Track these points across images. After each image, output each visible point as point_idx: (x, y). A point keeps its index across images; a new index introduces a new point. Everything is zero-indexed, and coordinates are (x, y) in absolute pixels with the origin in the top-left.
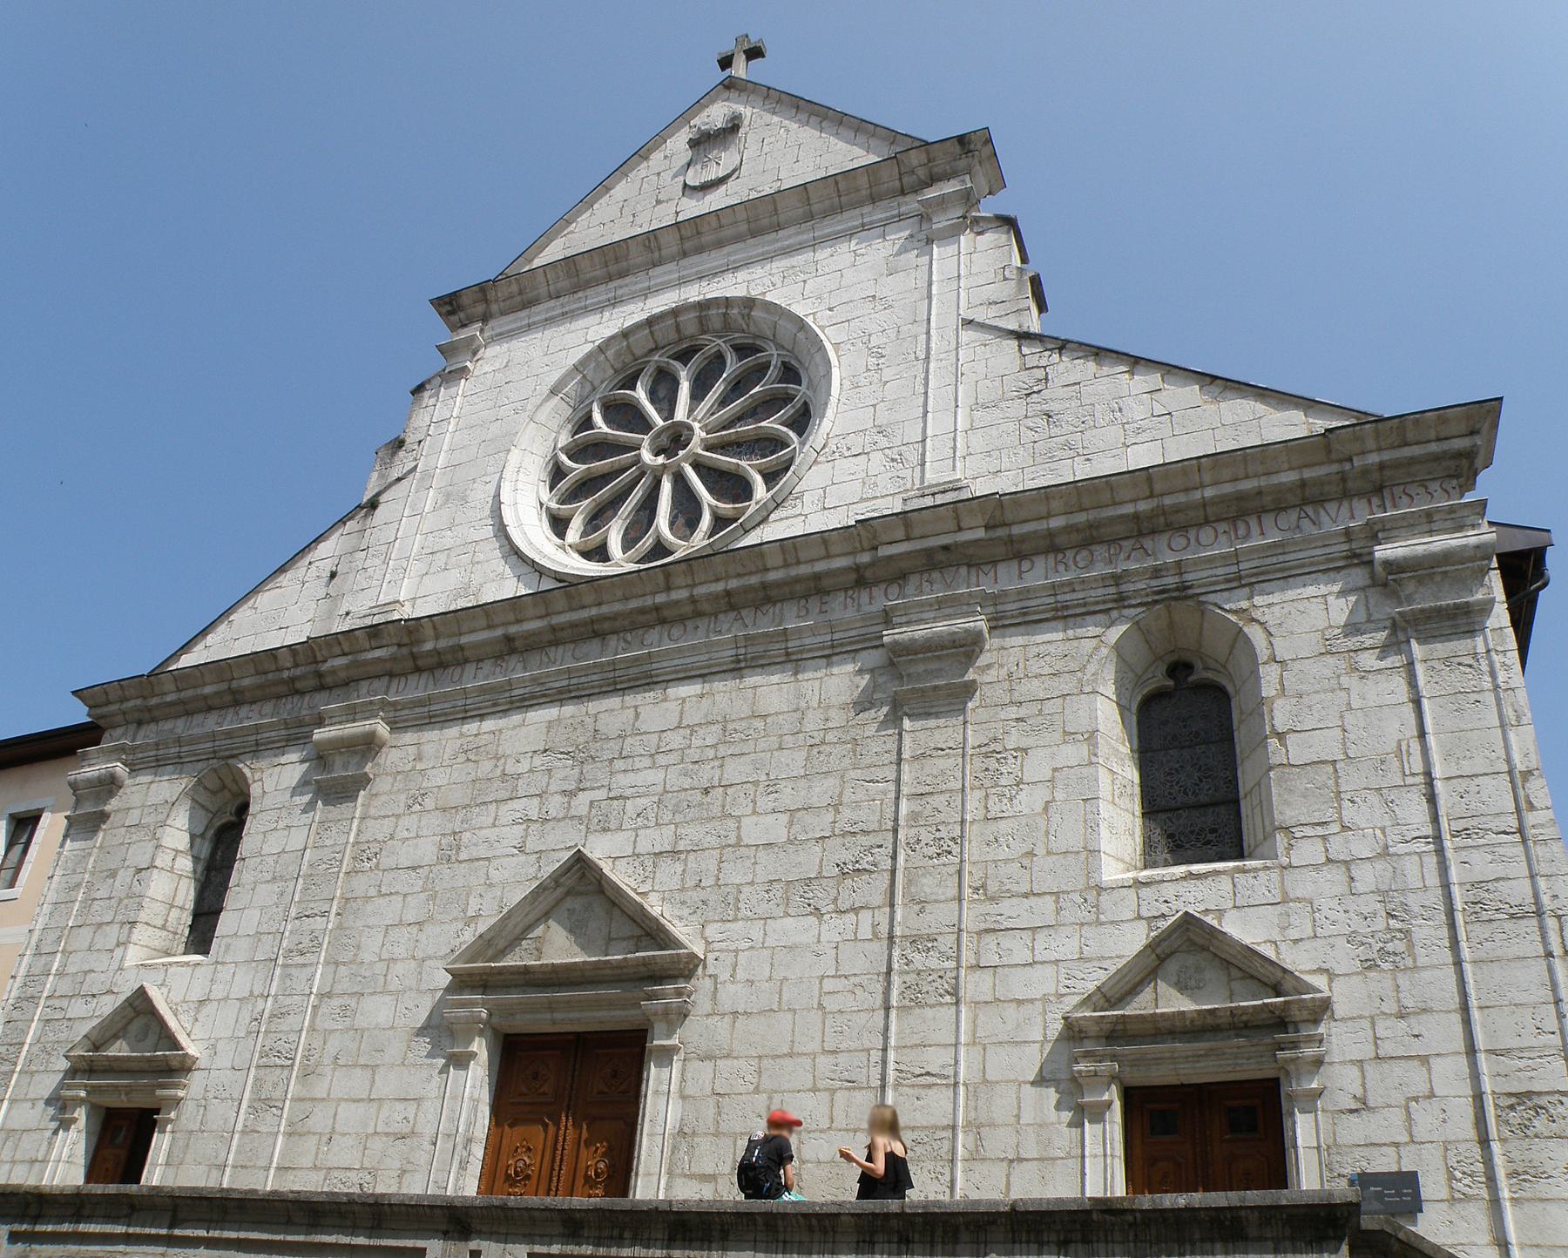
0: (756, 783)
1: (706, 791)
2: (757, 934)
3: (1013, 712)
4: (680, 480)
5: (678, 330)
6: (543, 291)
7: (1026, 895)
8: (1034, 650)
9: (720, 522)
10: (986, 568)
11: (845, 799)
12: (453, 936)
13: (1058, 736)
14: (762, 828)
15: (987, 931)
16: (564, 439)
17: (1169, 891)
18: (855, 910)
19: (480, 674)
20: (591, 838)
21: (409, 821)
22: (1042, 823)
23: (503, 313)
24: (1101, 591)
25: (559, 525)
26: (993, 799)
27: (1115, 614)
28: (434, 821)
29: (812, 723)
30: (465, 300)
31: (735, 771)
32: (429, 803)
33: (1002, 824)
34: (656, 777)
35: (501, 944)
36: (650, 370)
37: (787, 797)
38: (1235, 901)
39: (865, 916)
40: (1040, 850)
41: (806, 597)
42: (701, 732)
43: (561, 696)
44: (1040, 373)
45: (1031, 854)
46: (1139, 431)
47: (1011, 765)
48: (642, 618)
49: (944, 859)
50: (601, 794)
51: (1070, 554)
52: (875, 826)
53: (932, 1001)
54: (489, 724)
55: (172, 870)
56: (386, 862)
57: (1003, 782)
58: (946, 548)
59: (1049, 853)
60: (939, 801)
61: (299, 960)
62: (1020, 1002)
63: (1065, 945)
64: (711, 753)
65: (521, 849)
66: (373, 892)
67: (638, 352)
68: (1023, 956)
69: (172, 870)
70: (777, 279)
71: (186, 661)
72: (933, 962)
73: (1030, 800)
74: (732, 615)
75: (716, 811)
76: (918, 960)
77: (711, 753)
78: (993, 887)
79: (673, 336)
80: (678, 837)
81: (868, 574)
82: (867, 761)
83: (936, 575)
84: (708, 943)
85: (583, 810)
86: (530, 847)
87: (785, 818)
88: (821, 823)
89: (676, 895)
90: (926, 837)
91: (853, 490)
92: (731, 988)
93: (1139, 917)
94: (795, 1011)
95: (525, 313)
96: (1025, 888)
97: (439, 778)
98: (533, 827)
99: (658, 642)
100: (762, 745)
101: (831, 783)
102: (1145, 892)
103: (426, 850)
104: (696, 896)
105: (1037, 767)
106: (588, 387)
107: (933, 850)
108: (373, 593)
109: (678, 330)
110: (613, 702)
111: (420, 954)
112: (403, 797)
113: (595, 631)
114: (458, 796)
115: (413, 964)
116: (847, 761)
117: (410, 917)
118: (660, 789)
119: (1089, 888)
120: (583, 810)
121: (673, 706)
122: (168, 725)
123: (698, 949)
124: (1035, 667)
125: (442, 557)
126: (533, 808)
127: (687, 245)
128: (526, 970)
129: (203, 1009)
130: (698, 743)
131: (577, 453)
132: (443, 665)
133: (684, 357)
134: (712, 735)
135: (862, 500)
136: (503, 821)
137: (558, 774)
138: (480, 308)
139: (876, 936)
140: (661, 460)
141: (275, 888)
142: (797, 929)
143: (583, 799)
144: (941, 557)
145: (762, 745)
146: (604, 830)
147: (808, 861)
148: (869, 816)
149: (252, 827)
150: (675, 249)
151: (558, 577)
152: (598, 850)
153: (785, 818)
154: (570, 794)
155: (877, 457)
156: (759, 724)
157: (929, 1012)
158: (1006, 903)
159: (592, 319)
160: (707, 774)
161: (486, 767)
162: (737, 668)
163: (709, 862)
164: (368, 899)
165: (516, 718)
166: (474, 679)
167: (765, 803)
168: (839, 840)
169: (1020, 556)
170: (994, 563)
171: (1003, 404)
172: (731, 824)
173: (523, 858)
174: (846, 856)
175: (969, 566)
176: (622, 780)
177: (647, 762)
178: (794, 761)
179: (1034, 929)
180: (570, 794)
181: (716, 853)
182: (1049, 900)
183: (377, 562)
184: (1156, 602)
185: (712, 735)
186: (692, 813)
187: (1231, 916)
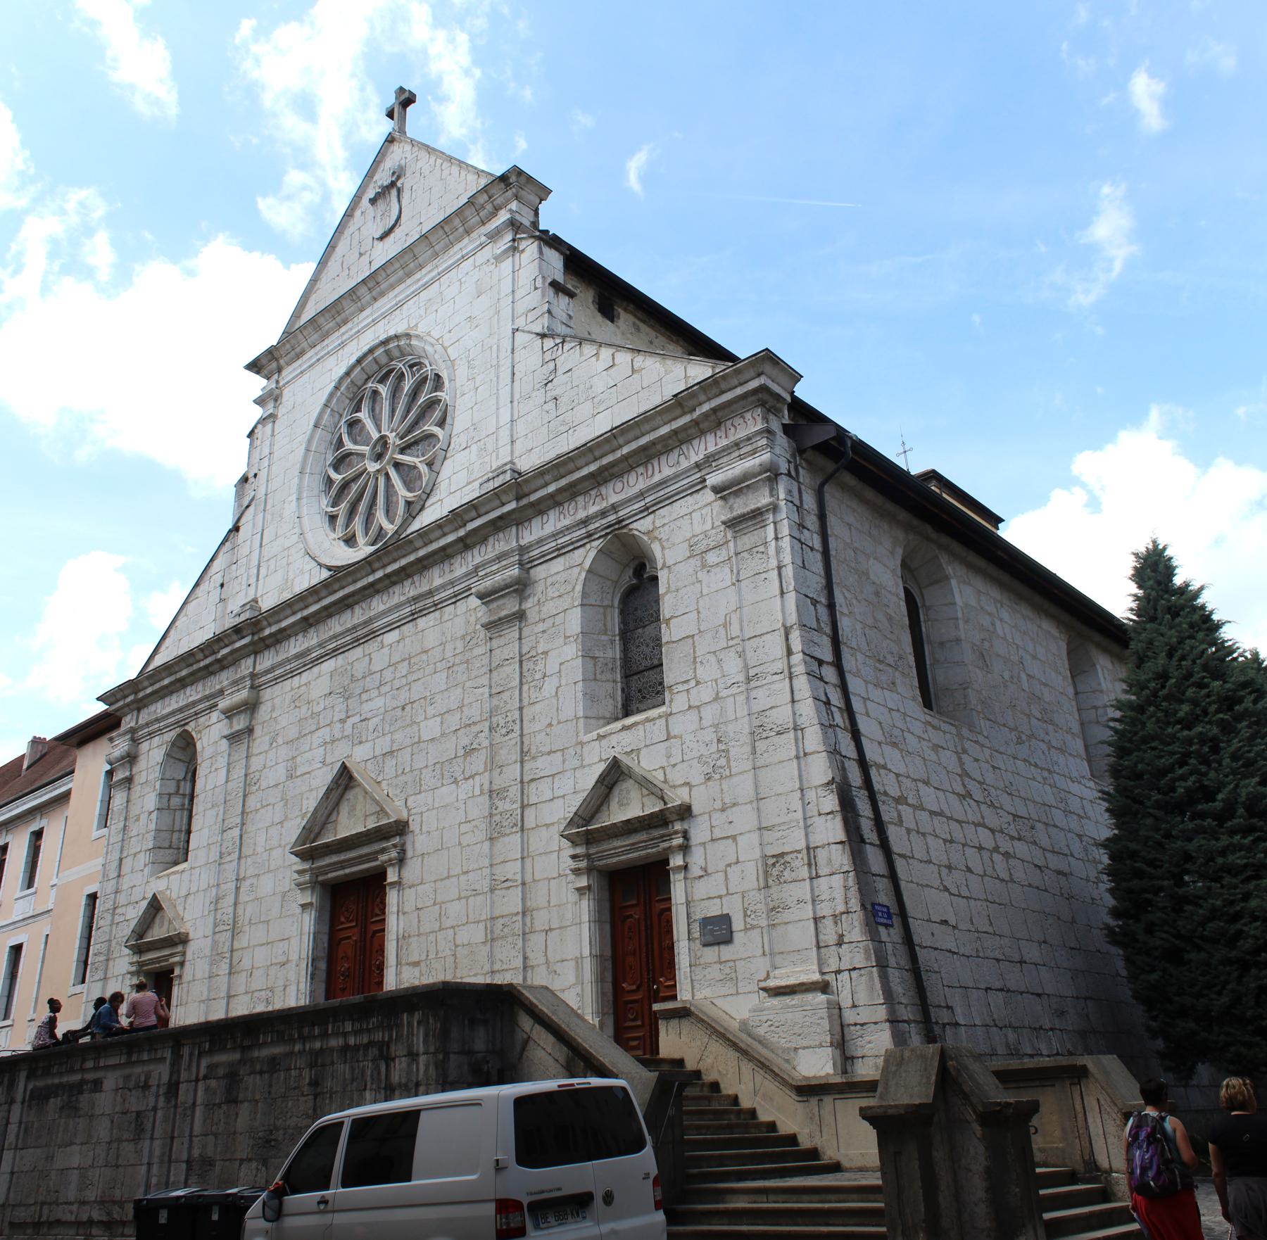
0: (425, 698)
1: (403, 709)
2: (430, 801)
3: (541, 627)
4: (397, 465)
5: (377, 363)
6: (305, 344)
7: (549, 753)
8: (550, 580)
9: (409, 503)
10: (526, 524)
11: (466, 702)
12: (293, 830)
13: (562, 639)
14: (430, 728)
15: (533, 780)
16: (330, 459)
17: (614, 739)
18: (472, 777)
19: (298, 643)
20: (355, 748)
21: (272, 754)
22: (554, 700)
23: (288, 364)
24: (579, 533)
25: (333, 518)
26: (532, 690)
27: (588, 546)
28: (284, 753)
29: (448, 654)
30: (264, 361)
31: (417, 691)
32: (280, 741)
33: (537, 706)
34: (379, 703)
35: (316, 829)
36: (368, 394)
37: (440, 706)
38: (646, 742)
39: (477, 778)
40: (555, 722)
41: (442, 562)
42: (399, 666)
43: (335, 653)
44: (551, 365)
45: (550, 725)
46: (600, 402)
47: (540, 666)
48: (367, 592)
49: (510, 736)
50: (357, 719)
51: (566, 505)
52: (478, 719)
53: (508, 831)
54: (306, 677)
55: (169, 808)
56: (264, 784)
57: (538, 676)
58: (500, 518)
59: (559, 723)
60: (506, 696)
61: (229, 859)
62: (547, 825)
63: (565, 785)
64: (404, 681)
65: (323, 763)
66: (259, 806)
67: (359, 383)
68: (548, 795)
69: (169, 808)
70: (422, 311)
71: (151, 667)
72: (508, 806)
73: (549, 687)
74: (410, 580)
75: (408, 719)
76: (500, 804)
77: (404, 681)
78: (533, 750)
79: (376, 367)
80: (393, 741)
81: (468, 541)
82: (474, 674)
83: (501, 535)
84: (409, 811)
85: (348, 731)
86: (328, 760)
87: (438, 719)
88: (454, 721)
89: (394, 781)
90: (502, 723)
91: (462, 478)
92: (420, 837)
93: (601, 760)
94: (448, 848)
95: (299, 362)
96: (547, 749)
97: (283, 721)
98: (329, 746)
99: (378, 605)
100: (427, 672)
101: (459, 690)
102: (604, 742)
103: (280, 773)
104: (402, 779)
105: (552, 667)
106: (337, 416)
107: (504, 731)
108: (242, 594)
109: (377, 363)
110: (358, 652)
111: (283, 843)
112: (267, 738)
113: (346, 604)
114: (293, 733)
115: (280, 850)
116: (465, 676)
117: (277, 820)
118: (382, 710)
119: (578, 743)
120: (348, 731)
121: (386, 650)
122: (152, 708)
123: (404, 816)
124: (552, 592)
125: (272, 561)
126: (324, 734)
127: (374, 293)
128: (327, 845)
129: (190, 895)
130: (398, 675)
131: (337, 466)
132: (279, 642)
133: (382, 381)
134: (403, 669)
135: (468, 484)
136: (315, 745)
137: (337, 709)
138: (274, 365)
139: (482, 793)
140: (377, 466)
141: (213, 812)
142: (447, 793)
143: (350, 722)
144: (500, 524)
145: (427, 672)
146: (361, 743)
147: (449, 748)
148: (474, 712)
149: (201, 772)
150: (368, 298)
151: (329, 568)
152: (358, 757)
153: (438, 719)
154: (343, 721)
155: (474, 448)
156: (424, 657)
157: (506, 839)
158: (540, 760)
159: (331, 361)
160: (404, 696)
161: (304, 709)
162: (414, 617)
163: (405, 756)
164: (257, 810)
165: (315, 670)
166: (295, 646)
167: (431, 711)
168: (463, 731)
169: (541, 513)
170: (530, 520)
171: (534, 394)
172: (415, 728)
173: (325, 769)
174: (466, 741)
175: (517, 525)
176: (367, 707)
177: (375, 693)
178: (440, 680)
179: (553, 776)
180: (343, 721)
181: (409, 749)
182: (559, 754)
183: (242, 571)
184: (607, 534)
185: (403, 669)
186: (399, 723)
187: (644, 752)
